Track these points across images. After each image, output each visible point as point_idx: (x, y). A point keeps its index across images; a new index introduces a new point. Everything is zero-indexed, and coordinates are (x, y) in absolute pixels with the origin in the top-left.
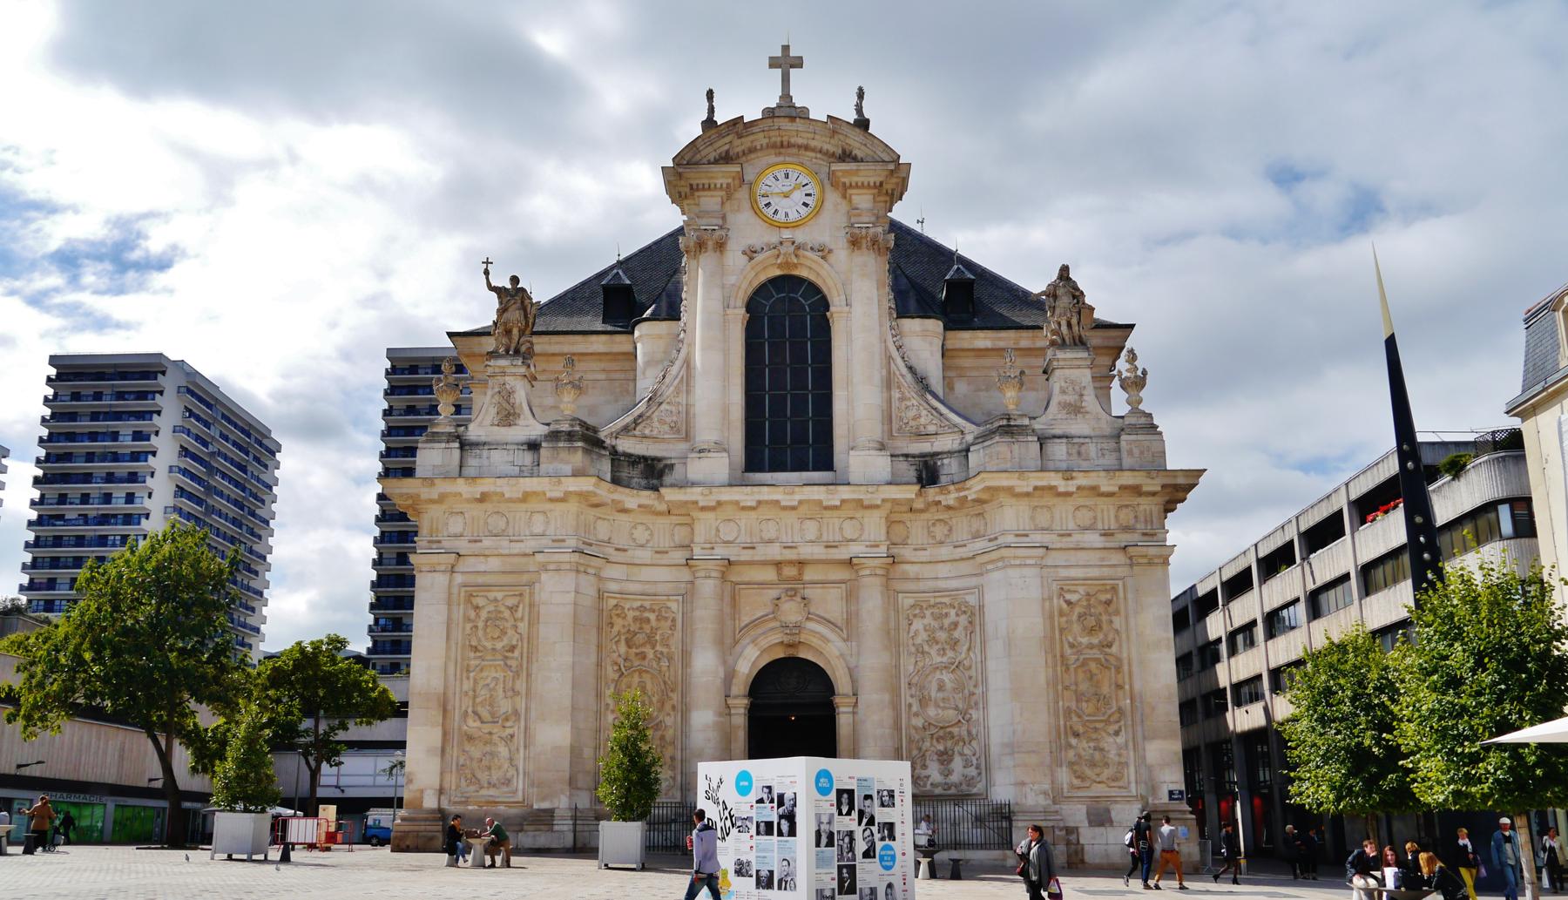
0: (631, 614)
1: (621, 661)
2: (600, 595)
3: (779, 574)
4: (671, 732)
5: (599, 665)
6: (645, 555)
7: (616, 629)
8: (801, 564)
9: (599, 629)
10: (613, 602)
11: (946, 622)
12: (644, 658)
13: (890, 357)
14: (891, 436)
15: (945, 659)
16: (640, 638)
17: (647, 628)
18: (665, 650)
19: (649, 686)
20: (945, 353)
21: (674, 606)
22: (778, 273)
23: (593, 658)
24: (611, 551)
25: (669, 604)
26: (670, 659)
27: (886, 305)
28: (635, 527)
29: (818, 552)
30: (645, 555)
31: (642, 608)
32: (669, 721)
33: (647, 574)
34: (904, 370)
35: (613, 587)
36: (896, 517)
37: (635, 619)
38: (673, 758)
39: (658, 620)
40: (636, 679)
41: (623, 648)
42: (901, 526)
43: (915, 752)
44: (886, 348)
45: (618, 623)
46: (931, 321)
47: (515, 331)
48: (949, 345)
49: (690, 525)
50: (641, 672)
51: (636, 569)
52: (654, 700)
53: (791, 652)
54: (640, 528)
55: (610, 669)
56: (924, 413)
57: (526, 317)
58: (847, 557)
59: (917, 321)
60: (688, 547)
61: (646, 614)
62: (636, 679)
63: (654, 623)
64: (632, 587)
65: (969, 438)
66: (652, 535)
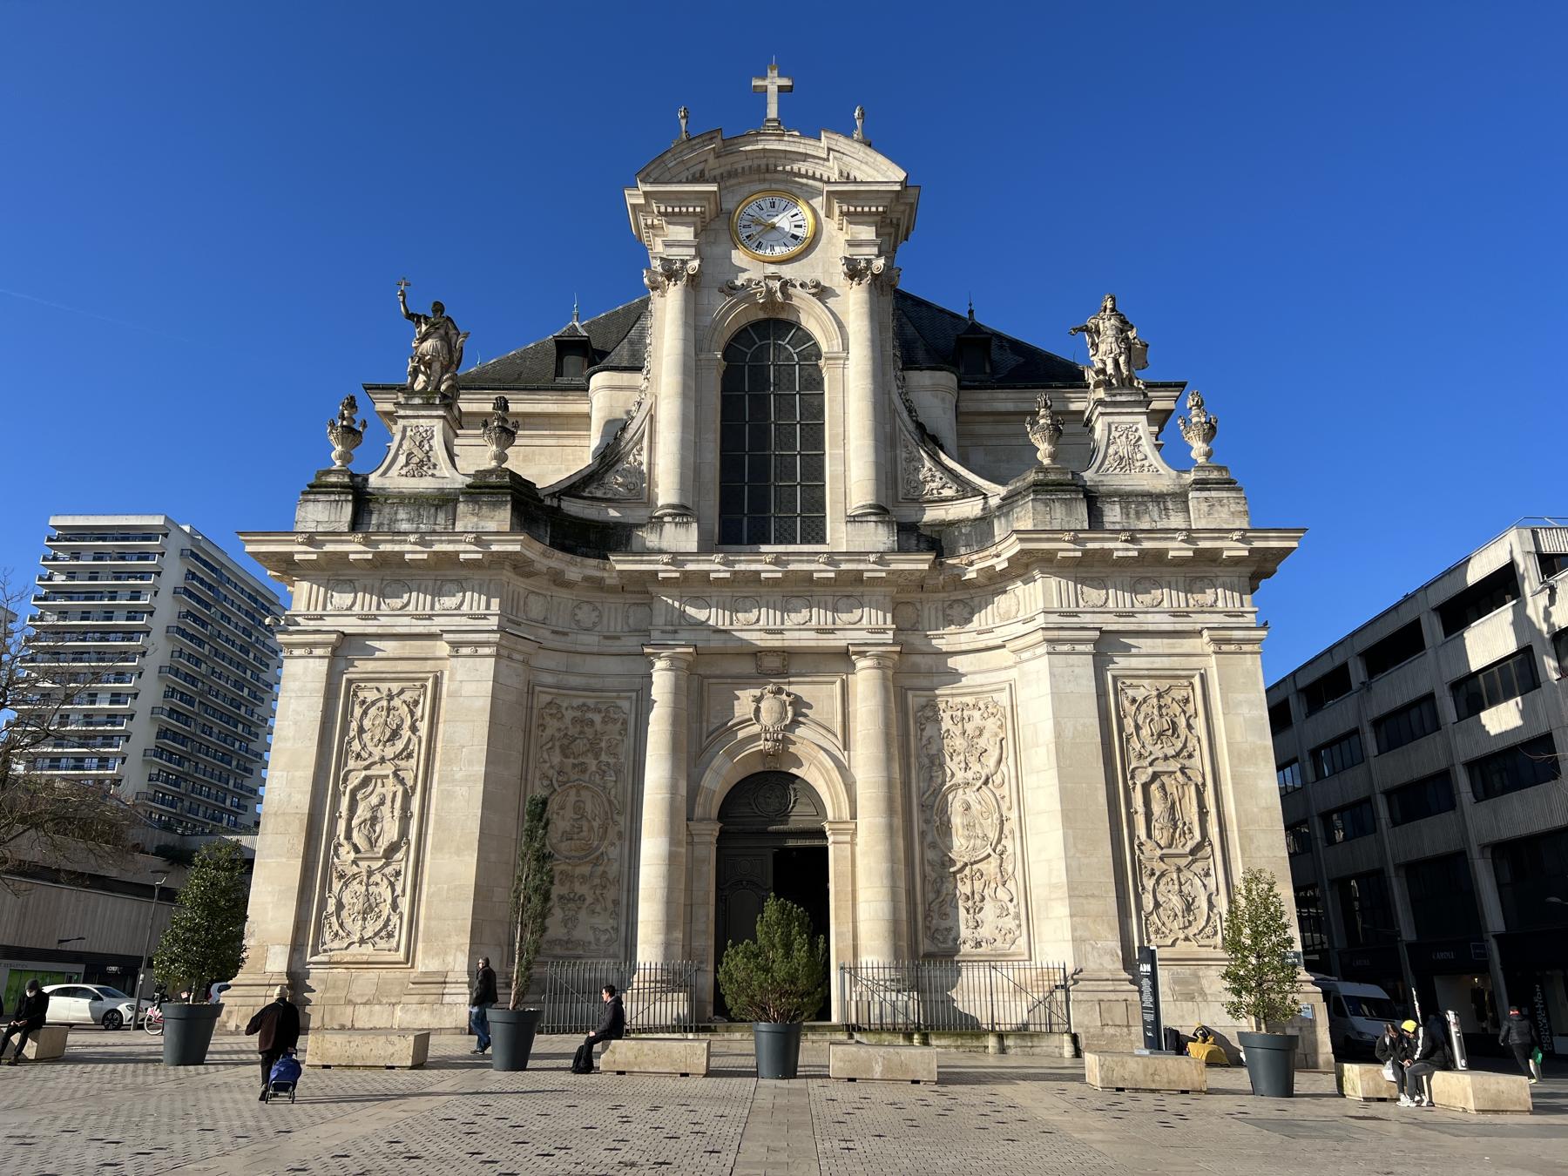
0: (569, 715)
1: (551, 772)
2: (530, 690)
3: (758, 666)
4: (615, 866)
5: (524, 778)
6: (590, 641)
7: (549, 732)
8: (787, 654)
9: (527, 733)
10: (548, 698)
11: (970, 727)
12: (584, 771)
13: (895, 410)
14: (896, 502)
15: (970, 775)
16: (580, 745)
17: (589, 731)
18: (612, 761)
19: (589, 807)
20: (958, 413)
21: (625, 705)
22: (762, 315)
23: (516, 769)
24: (547, 634)
25: (620, 703)
26: (618, 772)
27: (890, 351)
28: (578, 607)
29: (808, 639)
30: (590, 641)
31: (584, 708)
32: (613, 852)
33: (592, 664)
34: (911, 427)
35: (548, 679)
36: (905, 597)
37: (575, 721)
38: (616, 903)
39: (604, 722)
40: (572, 797)
41: (557, 759)
42: (910, 609)
43: (931, 896)
44: (891, 401)
45: (553, 726)
46: (944, 373)
47: (437, 366)
48: (964, 406)
49: (649, 606)
50: (579, 789)
51: (578, 658)
52: (596, 824)
53: (772, 765)
54: (586, 608)
55: (537, 782)
56: (938, 474)
57: (450, 351)
58: (843, 643)
59: (927, 373)
60: (647, 633)
61: (590, 715)
62: (572, 797)
63: (598, 726)
64: (574, 681)
65: (994, 502)
66: (600, 616)
